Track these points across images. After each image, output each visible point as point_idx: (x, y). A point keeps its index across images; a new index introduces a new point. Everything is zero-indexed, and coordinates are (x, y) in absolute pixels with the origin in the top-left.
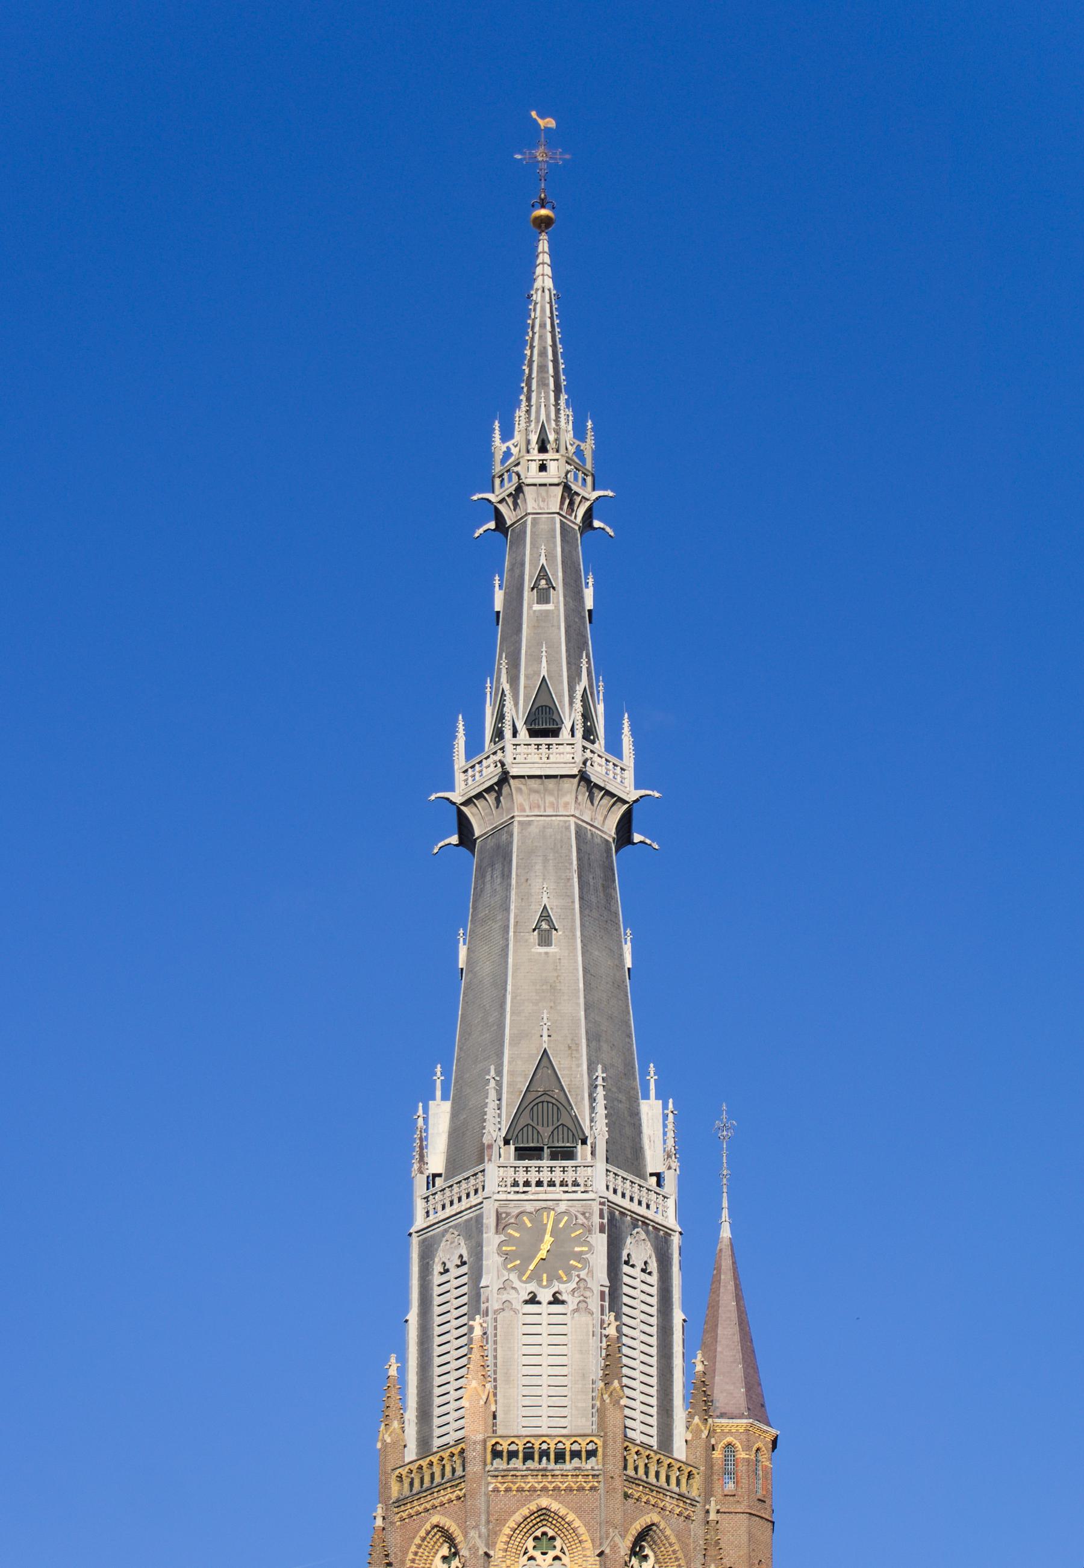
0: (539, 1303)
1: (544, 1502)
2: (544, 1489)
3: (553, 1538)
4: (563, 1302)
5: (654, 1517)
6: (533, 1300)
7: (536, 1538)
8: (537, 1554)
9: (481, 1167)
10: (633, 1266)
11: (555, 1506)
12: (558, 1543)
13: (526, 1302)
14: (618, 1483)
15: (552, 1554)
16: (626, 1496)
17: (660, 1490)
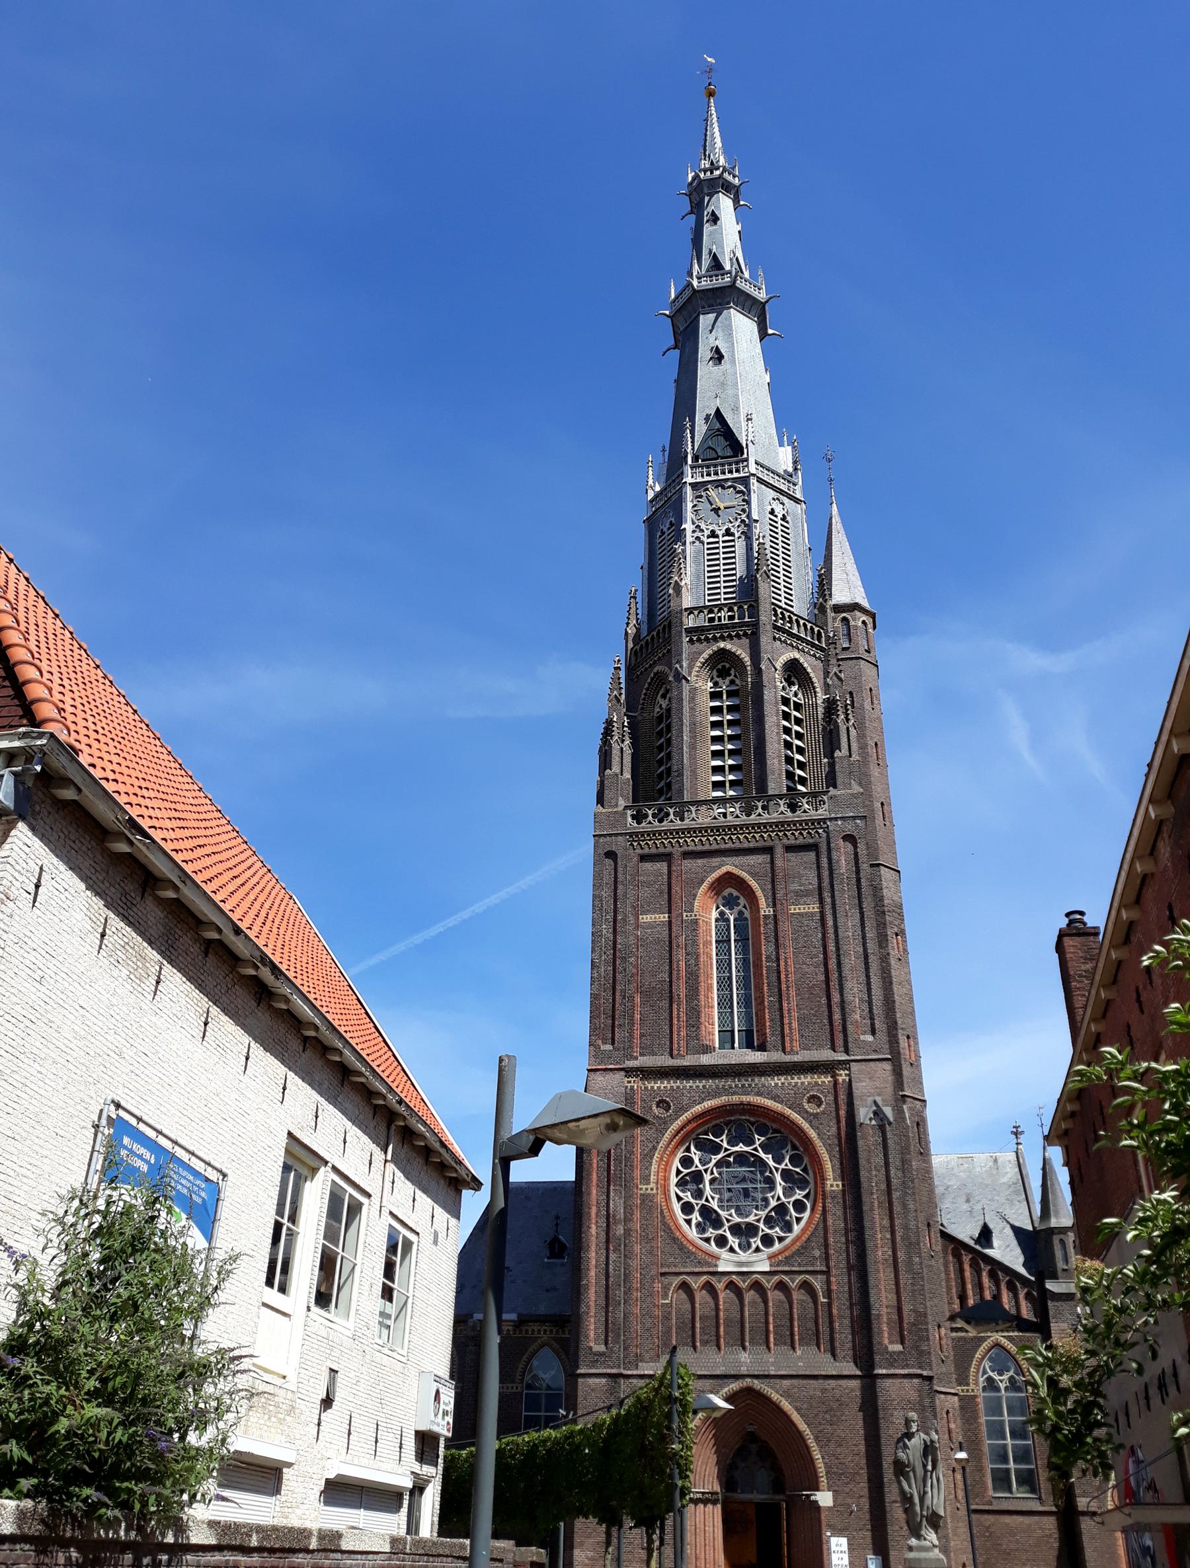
0: (717, 536)
1: (722, 645)
2: (723, 638)
3: (729, 669)
4: (733, 535)
5: (797, 655)
6: (713, 534)
7: (718, 671)
8: (719, 680)
9: (679, 472)
10: (776, 516)
11: (729, 647)
12: (732, 672)
13: (708, 537)
14: (769, 627)
15: (728, 679)
16: (775, 638)
17: (799, 638)
